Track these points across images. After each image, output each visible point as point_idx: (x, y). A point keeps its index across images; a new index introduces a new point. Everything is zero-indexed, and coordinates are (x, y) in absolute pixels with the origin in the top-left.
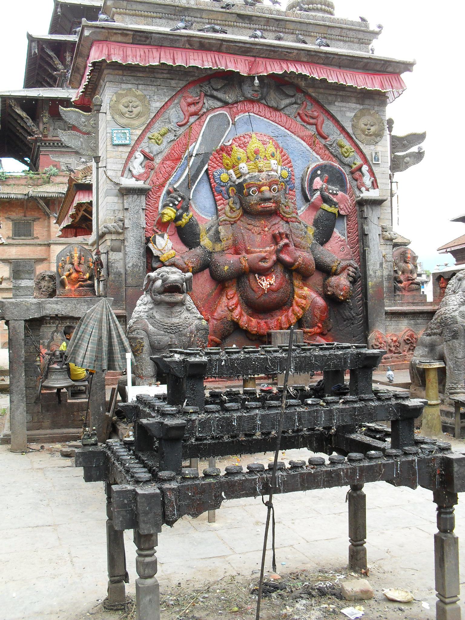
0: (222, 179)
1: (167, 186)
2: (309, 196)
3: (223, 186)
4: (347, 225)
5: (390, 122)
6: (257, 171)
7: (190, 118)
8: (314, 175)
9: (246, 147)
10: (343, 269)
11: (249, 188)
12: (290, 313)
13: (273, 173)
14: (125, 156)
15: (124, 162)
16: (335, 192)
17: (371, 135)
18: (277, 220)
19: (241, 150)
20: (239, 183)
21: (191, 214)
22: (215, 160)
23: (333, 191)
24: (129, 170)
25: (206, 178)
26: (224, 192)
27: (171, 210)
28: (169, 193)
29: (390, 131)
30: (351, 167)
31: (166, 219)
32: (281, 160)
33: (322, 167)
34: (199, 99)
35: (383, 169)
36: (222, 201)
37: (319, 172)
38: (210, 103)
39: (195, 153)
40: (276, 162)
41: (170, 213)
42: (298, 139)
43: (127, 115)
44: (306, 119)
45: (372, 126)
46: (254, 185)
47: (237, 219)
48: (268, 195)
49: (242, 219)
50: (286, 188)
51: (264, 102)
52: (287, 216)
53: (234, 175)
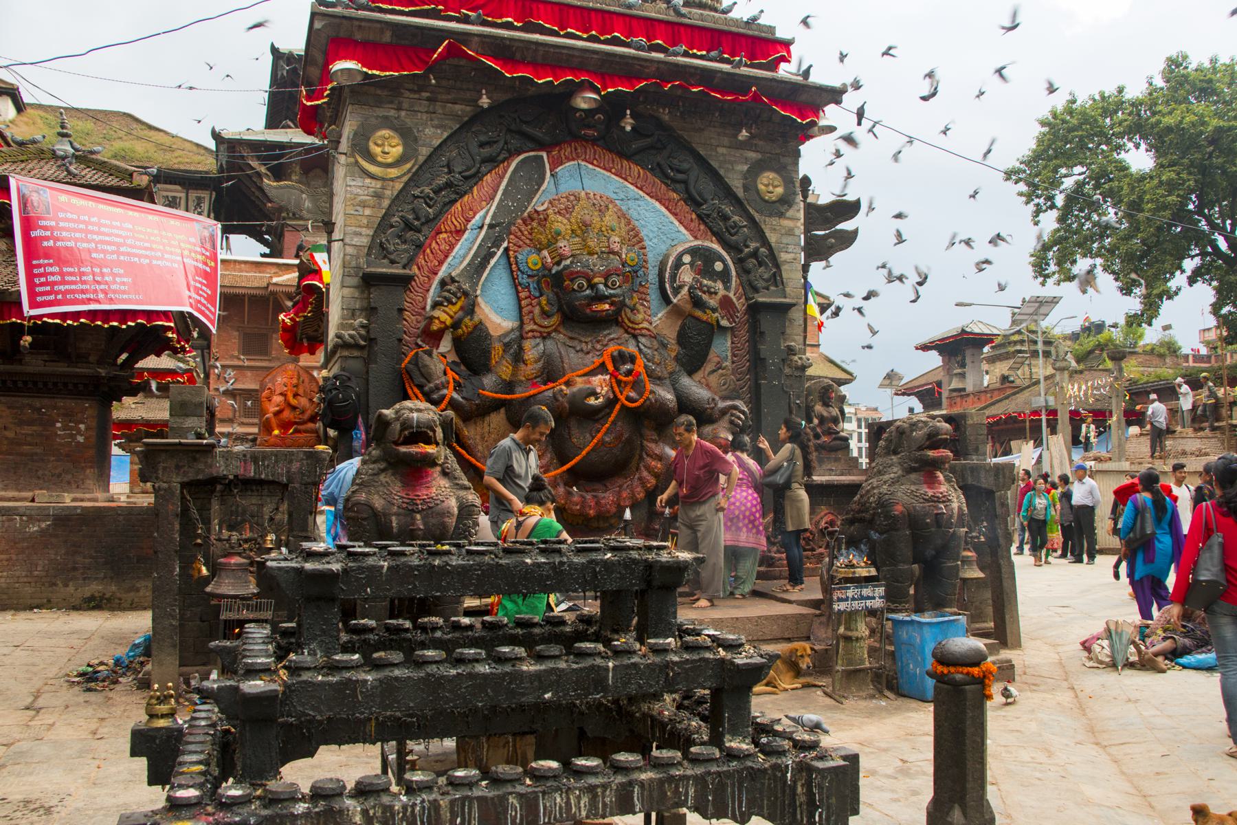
1: (441, 274)
5: (806, 181)
8: (678, 264)
10: (724, 412)
12: (636, 482)
18: (616, 333)
19: (560, 218)
20: (557, 272)
24: (381, 245)
25: (503, 261)
28: (443, 283)
29: (805, 196)
30: (741, 251)
31: (435, 326)
33: (693, 252)
35: (792, 256)
37: (687, 259)
38: (515, 142)
39: (488, 221)
41: (443, 316)
42: (657, 204)
43: (379, 159)
46: (579, 275)
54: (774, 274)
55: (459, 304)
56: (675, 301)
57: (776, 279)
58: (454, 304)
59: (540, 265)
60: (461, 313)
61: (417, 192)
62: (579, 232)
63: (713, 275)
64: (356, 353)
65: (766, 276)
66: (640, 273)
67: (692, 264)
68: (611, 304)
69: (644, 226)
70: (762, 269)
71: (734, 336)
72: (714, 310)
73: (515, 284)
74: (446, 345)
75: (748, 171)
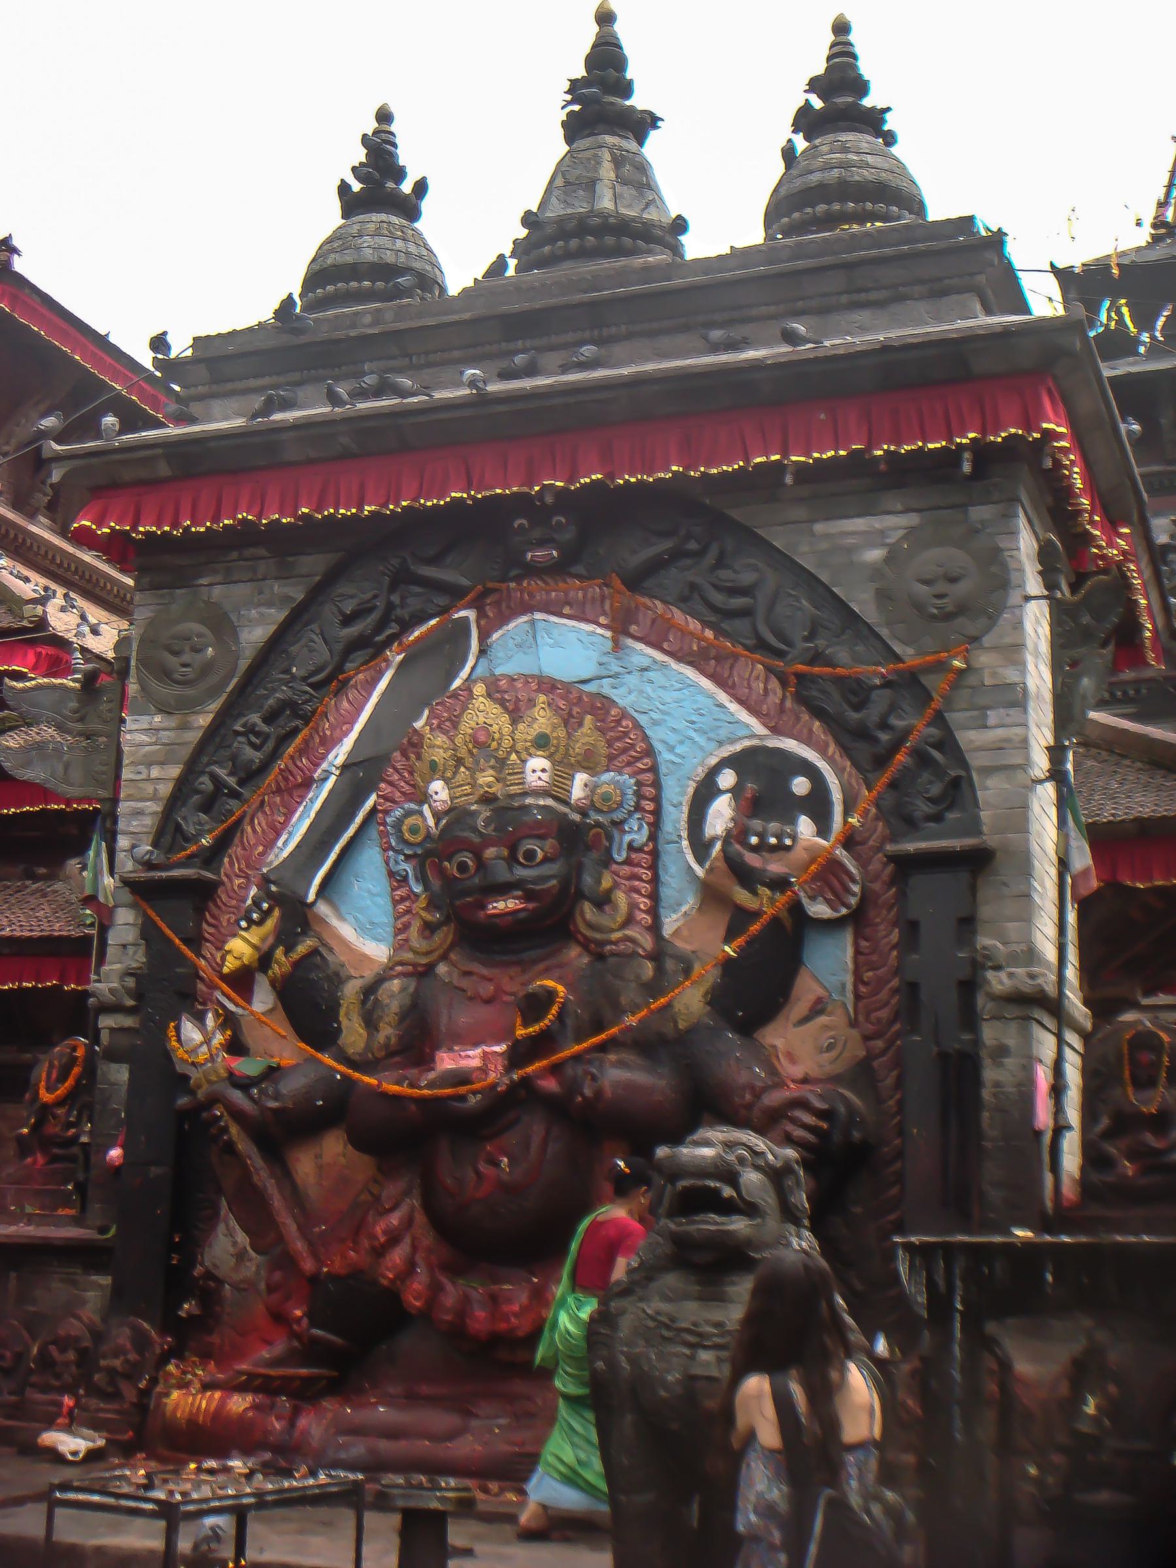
4: (858, 952)
8: (706, 792)
9: (455, 725)
15: (159, 809)
16: (773, 840)
17: (948, 617)
19: (441, 739)
21: (301, 949)
22: (396, 777)
23: (762, 836)
30: (875, 740)
31: (230, 965)
32: (603, 750)
34: (375, 597)
35: (1000, 732)
36: (407, 904)
37: (727, 779)
39: (340, 760)
40: (545, 763)
41: (240, 948)
42: (690, 672)
43: (177, 676)
44: (718, 598)
45: (953, 580)
47: (436, 955)
48: (502, 873)
51: (580, 569)
53: (431, 822)
54: (956, 783)
55: (270, 924)
56: (700, 871)
57: (958, 791)
58: (260, 923)
59: (423, 833)
60: (271, 940)
61: (238, 728)
62: (469, 761)
63: (789, 807)
64: (128, 1022)
65: (936, 790)
66: (634, 824)
67: (736, 791)
68: (529, 896)
69: (655, 723)
70: (926, 776)
71: (857, 936)
72: (780, 884)
73: (391, 874)
74: (263, 999)
75: (888, 560)
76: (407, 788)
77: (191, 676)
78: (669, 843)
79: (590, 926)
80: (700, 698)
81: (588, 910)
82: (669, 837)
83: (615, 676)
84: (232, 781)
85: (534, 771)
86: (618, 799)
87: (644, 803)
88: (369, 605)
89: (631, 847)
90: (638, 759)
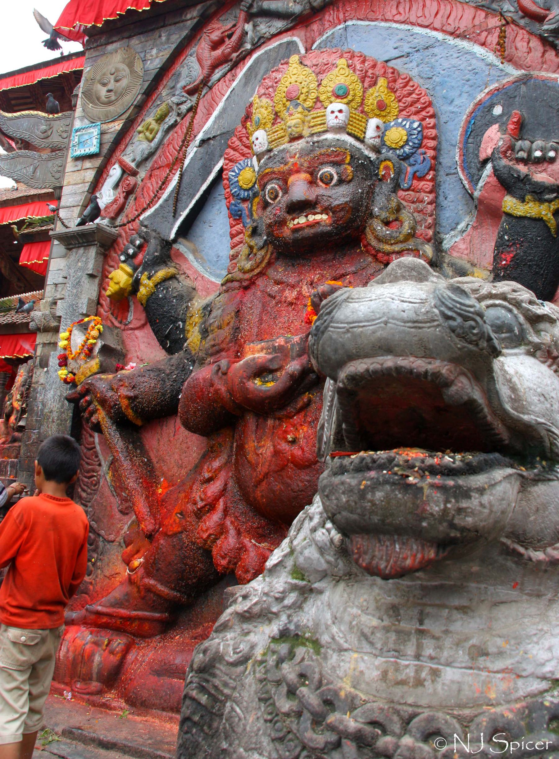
0: (241, 183)
2: (465, 182)
3: (244, 200)
6: (287, 139)
7: (217, 71)
11: (263, 187)
13: (329, 136)
14: (90, 175)
21: (161, 273)
22: (238, 143)
26: (246, 212)
27: (123, 269)
34: (234, 26)
36: (241, 236)
40: (343, 107)
49: (271, 272)
50: (399, 172)
52: (387, 248)
61: (140, 128)
76: (246, 150)
77: (113, 98)
78: (447, 175)
79: (379, 240)
80: (474, 61)
81: (379, 227)
82: (448, 171)
83: (408, 55)
84: (133, 165)
85: (333, 112)
86: (405, 138)
87: (426, 141)
88: (230, 32)
89: (415, 177)
90: (423, 109)
